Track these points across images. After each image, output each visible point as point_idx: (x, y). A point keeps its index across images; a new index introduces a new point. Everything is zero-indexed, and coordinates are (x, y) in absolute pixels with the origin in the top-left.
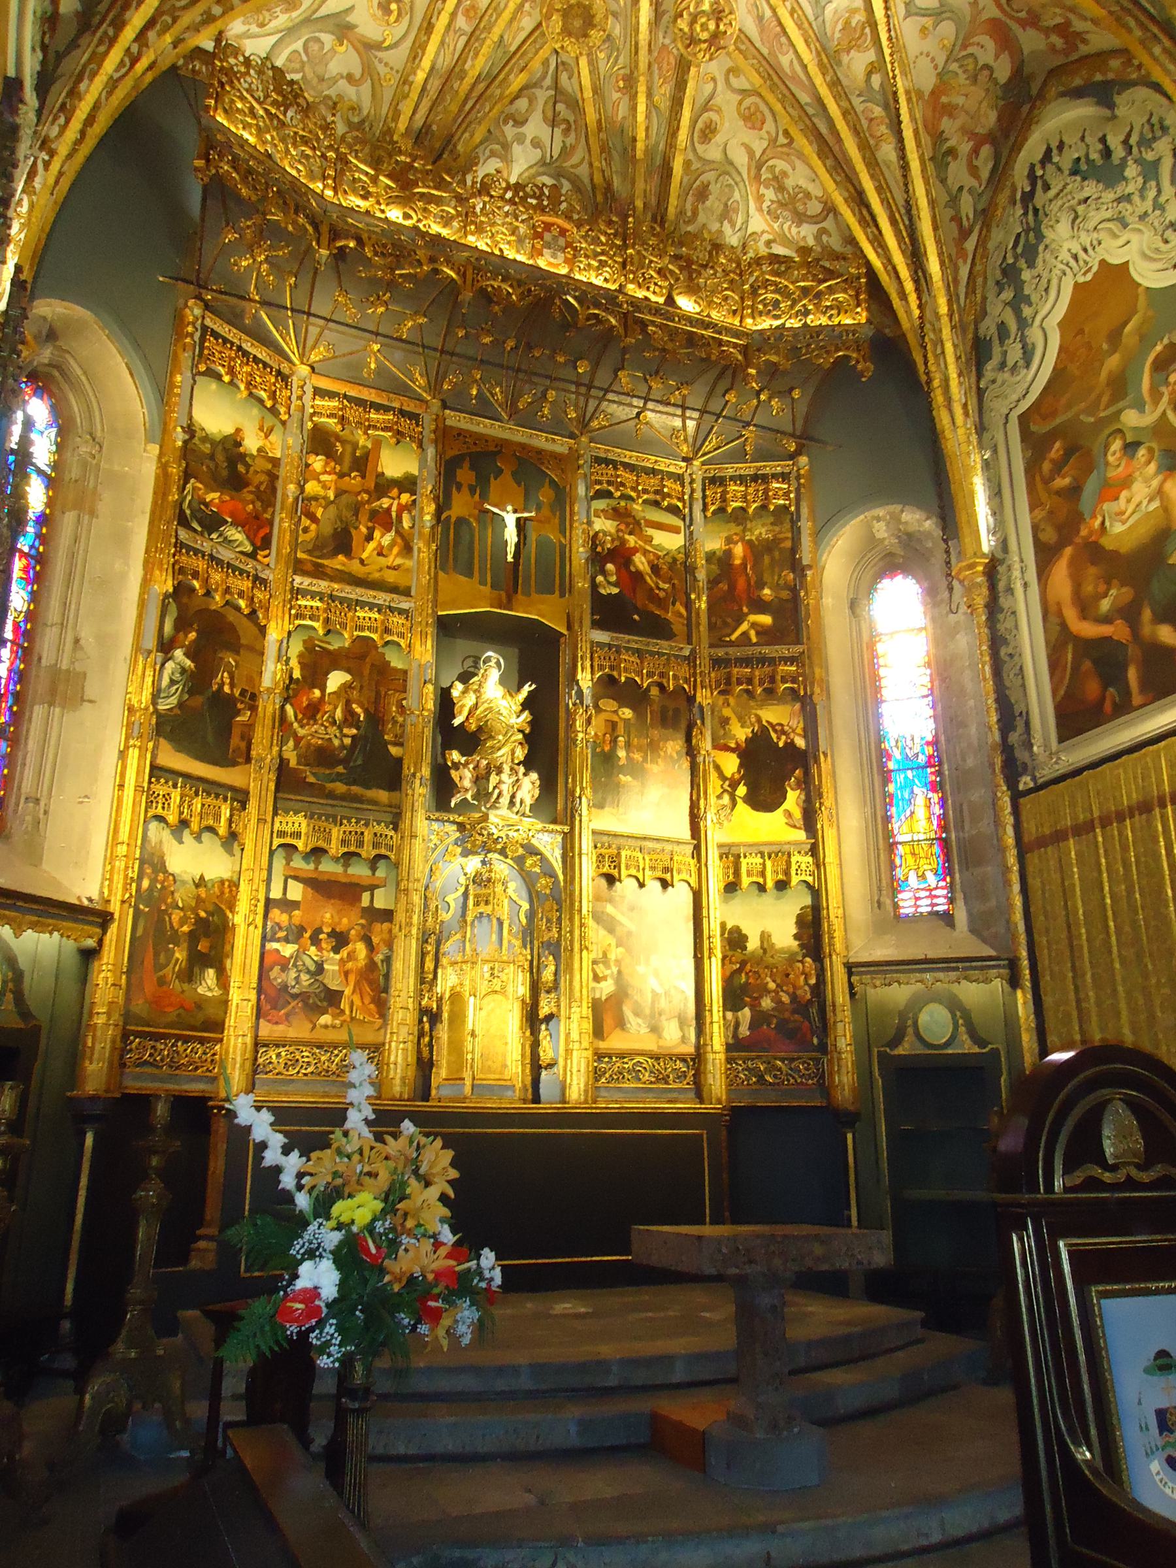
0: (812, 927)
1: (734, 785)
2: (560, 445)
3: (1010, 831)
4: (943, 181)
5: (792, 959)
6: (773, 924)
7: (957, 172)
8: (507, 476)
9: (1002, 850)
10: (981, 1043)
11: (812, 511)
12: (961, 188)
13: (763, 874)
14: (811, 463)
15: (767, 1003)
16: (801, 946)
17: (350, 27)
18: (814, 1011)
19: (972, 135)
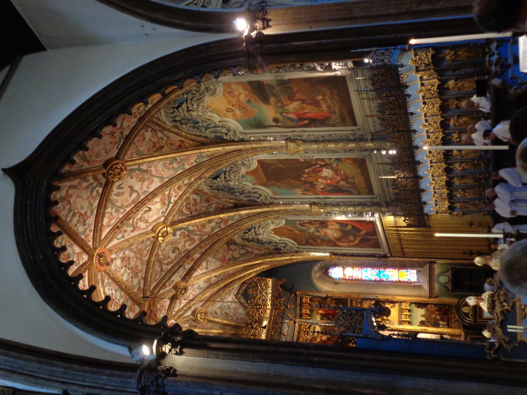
0: (420, 305)
1: (384, 319)
3: (400, 259)
4: (239, 258)
5: (427, 310)
6: (419, 313)
7: (236, 255)
9: (404, 261)
10: (449, 270)
11: (312, 291)
13: (406, 315)
14: (299, 291)
15: (438, 317)
16: (425, 307)
18: (440, 307)
19: (228, 251)
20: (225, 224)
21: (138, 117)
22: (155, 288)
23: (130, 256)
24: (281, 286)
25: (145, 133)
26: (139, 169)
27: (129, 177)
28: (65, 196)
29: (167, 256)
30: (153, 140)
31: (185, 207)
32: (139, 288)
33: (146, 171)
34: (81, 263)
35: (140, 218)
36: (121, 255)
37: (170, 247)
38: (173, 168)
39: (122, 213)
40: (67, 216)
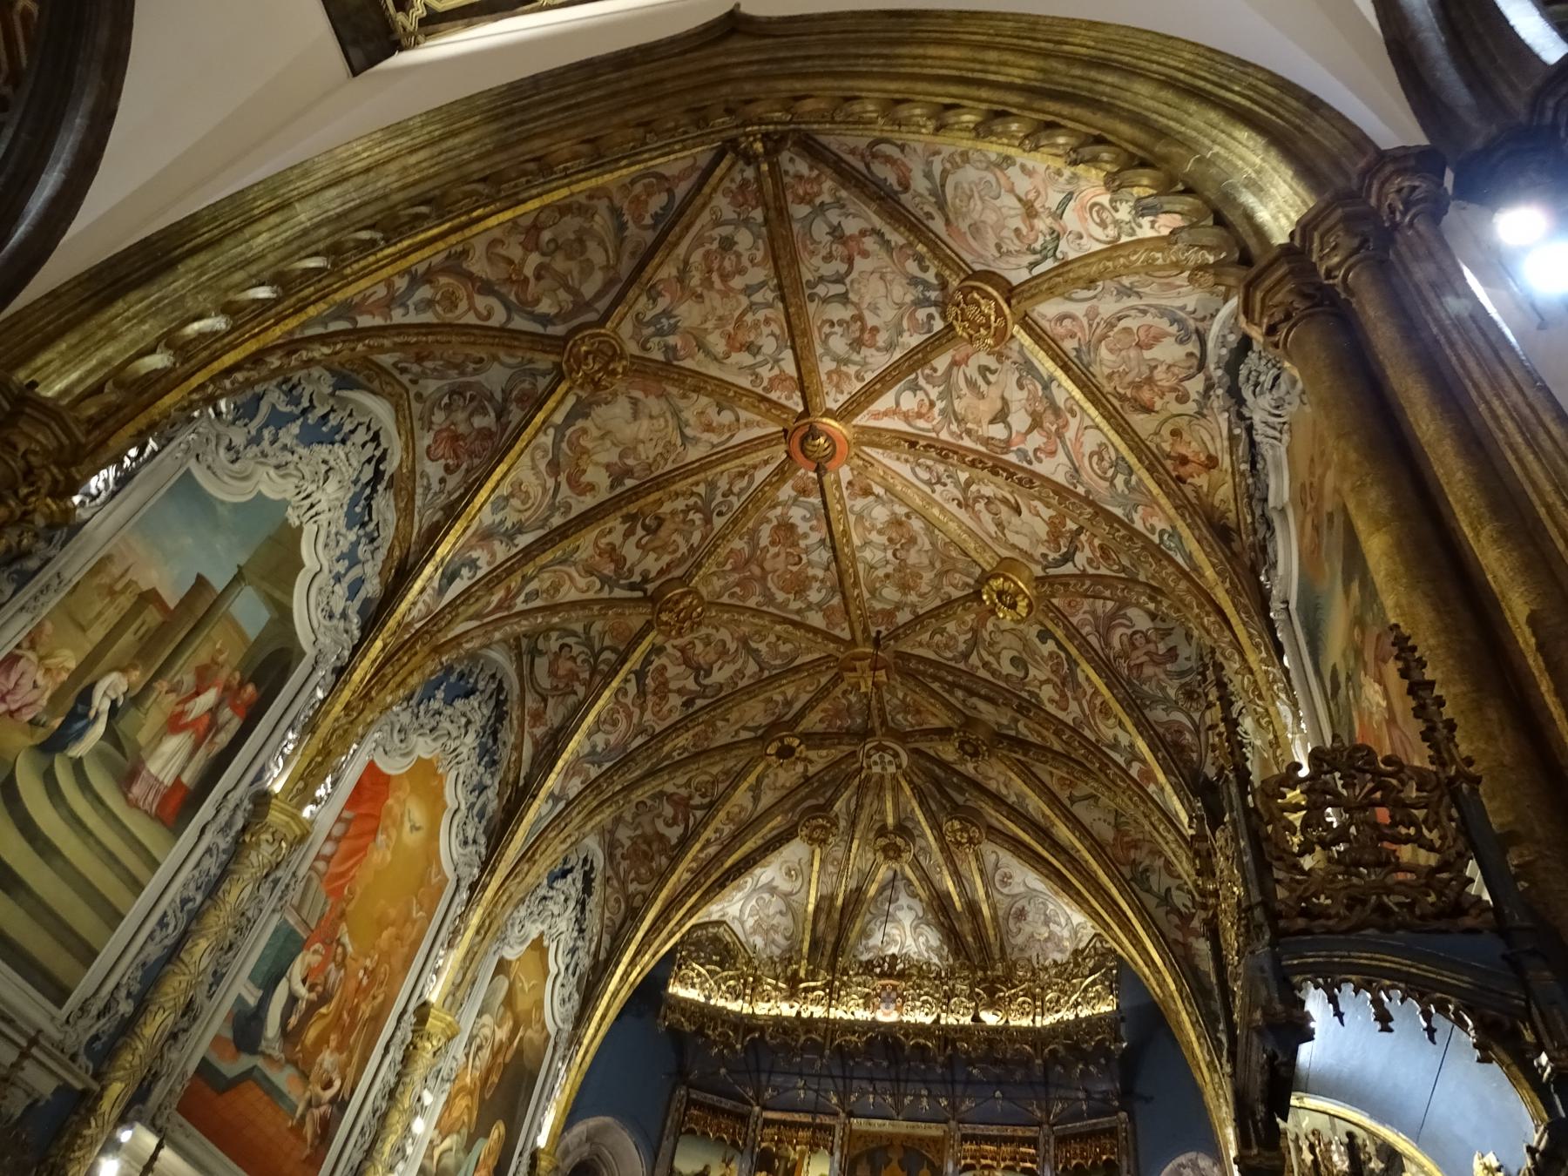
2: (935, 1131)
4: (1149, 890)
8: (895, 1164)
12: (1168, 890)
17: (775, 888)
20: (1140, 772)
21: (1112, 232)
22: (921, 659)
23: (919, 541)
24: (1104, 1040)
25: (1170, 340)
26: (1046, 387)
27: (1017, 375)
28: (851, 237)
29: (996, 649)
30: (1159, 374)
31: (1129, 632)
32: (889, 615)
33: (1056, 411)
34: (773, 396)
35: (989, 501)
36: (901, 510)
37: (1017, 644)
38: (1111, 481)
39: (952, 433)
40: (821, 279)
